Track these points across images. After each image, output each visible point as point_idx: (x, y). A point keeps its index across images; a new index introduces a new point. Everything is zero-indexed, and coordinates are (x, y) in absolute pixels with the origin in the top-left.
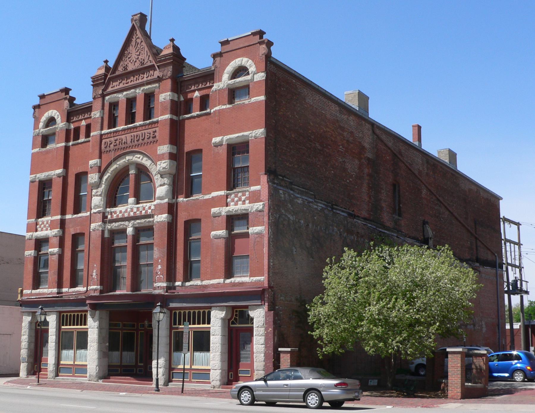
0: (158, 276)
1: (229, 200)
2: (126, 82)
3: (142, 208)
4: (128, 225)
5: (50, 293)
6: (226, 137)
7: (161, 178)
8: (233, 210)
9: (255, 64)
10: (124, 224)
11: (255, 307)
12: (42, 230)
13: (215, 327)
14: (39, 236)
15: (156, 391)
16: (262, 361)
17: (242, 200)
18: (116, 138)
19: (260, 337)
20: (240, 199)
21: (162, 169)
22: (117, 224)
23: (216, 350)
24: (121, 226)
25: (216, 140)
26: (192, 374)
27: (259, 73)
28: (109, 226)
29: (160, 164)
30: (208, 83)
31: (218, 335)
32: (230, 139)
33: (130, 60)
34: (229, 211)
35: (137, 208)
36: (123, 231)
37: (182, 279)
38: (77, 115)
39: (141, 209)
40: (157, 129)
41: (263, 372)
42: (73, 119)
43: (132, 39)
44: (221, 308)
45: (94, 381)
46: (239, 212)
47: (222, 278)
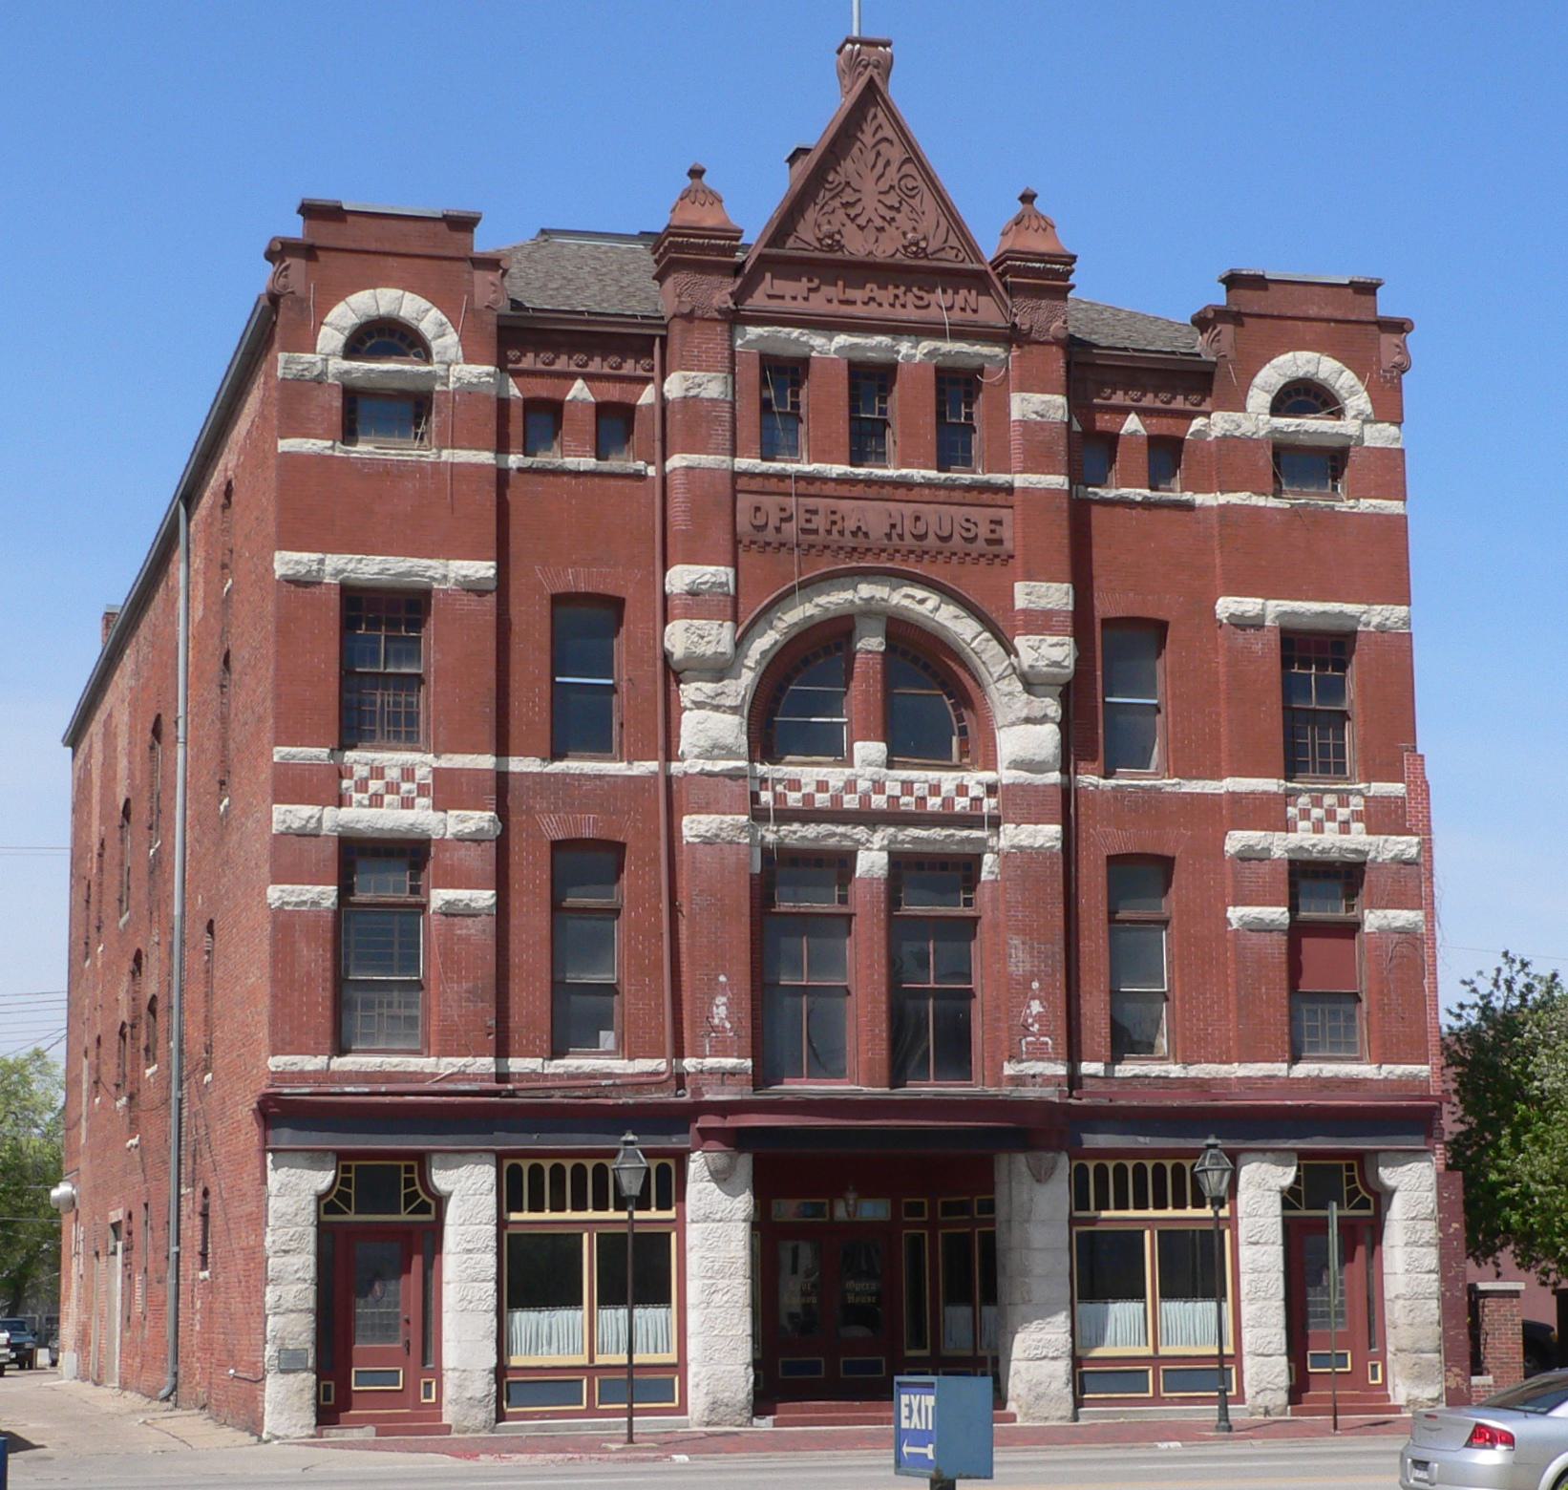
0: (1030, 1039)
1: (1292, 811)
2: (842, 297)
3: (927, 785)
4: (868, 841)
5: (451, 1074)
6: (1278, 606)
7: (1026, 695)
8: (1314, 846)
9: (1367, 389)
10: (844, 836)
11: (1400, 1156)
12: (376, 801)
13: (1260, 1216)
14: (359, 826)
15: (1217, 1428)
16: (1431, 1323)
17: (1340, 818)
18: (811, 503)
19: (1424, 1250)
20: (1331, 815)
21: (1047, 665)
22: (812, 831)
23: (1266, 1292)
24: (832, 842)
25: (1227, 606)
26: (1161, 1373)
27: (1382, 422)
28: (770, 834)
29: (1037, 644)
30: (1180, 398)
31: (1273, 1243)
32: (1294, 614)
33: (853, 212)
34: (1301, 847)
35: (903, 782)
36: (844, 861)
37: (1106, 1052)
39: (920, 789)
40: (1005, 514)
41: (1437, 1355)
42: (518, 361)
43: (859, 134)
44: (1280, 1157)
45: (730, 1425)
46: (1334, 855)
47: (1283, 1061)
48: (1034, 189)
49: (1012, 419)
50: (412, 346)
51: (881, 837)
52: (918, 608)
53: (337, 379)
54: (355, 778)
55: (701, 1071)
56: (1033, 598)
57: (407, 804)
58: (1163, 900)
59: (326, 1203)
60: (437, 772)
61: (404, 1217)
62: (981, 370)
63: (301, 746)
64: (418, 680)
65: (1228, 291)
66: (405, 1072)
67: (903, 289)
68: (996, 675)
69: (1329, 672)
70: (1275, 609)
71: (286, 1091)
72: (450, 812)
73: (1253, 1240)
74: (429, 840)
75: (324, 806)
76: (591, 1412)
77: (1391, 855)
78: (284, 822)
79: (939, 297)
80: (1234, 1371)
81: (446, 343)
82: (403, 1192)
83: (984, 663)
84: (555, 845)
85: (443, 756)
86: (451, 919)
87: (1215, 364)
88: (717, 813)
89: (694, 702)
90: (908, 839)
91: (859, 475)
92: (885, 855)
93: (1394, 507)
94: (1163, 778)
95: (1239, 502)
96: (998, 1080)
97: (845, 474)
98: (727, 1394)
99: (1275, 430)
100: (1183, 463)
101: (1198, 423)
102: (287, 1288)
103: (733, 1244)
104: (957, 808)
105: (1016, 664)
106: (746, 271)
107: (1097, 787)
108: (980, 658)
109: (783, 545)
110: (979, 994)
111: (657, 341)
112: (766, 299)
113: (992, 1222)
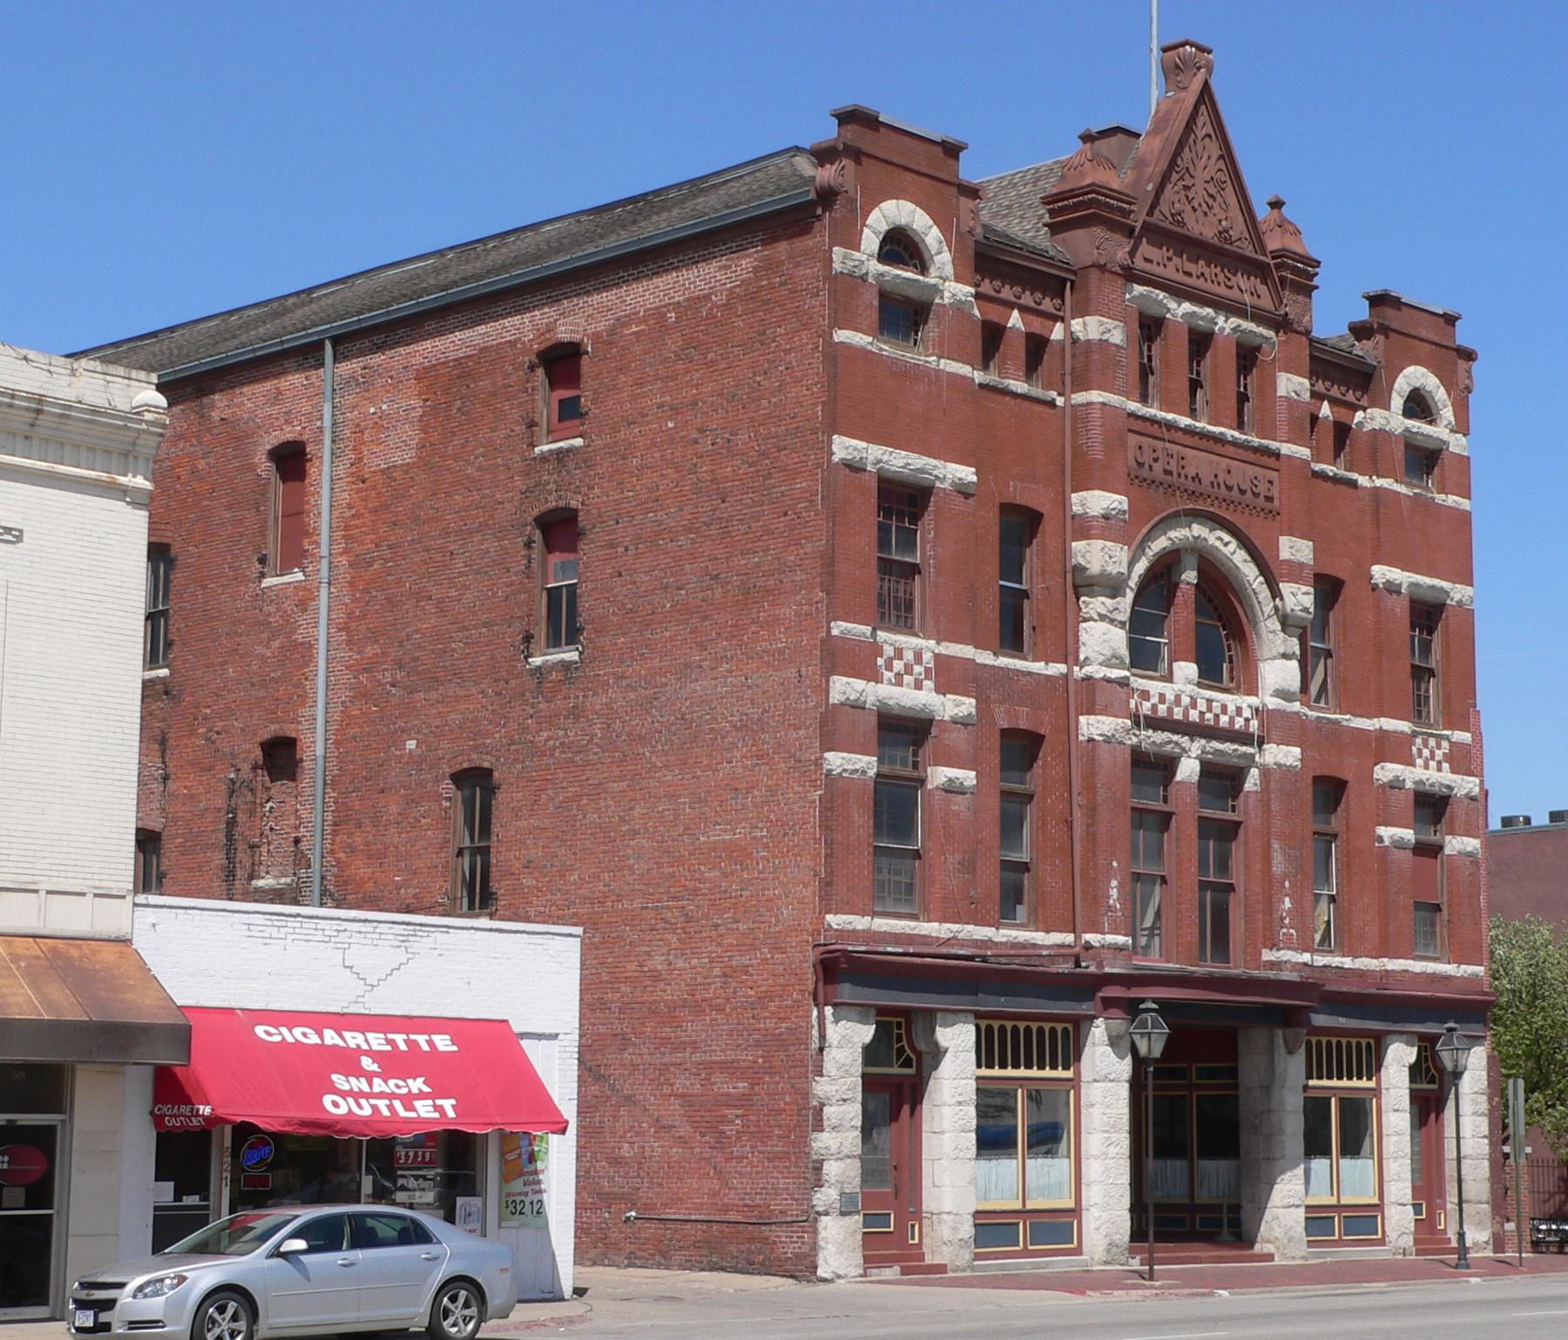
10: (1177, 743)
12: (899, 683)
14: (891, 702)
21: (1301, 610)
24: (1169, 748)
25: (1381, 573)
38: (1018, 284)
39: (1216, 707)
48: (1283, 198)
49: (1278, 394)
50: (912, 257)
51: (1196, 747)
52: (1222, 548)
53: (875, 278)
54: (885, 657)
55: (1103, 946)
56: (1293, 551)
57: (918, 685)
58: (1333, 817)
59: (871, 1054)
60: (938, 657)
61: (896, 1070)
62: (1258, 348)
63: (854, 623)
64: (914, 570)
65: (1370, 307)
66: (918, 935)
67: (1219, 268)
68: (1266, 614)
69: (1424, 636)
70: (1403, 577)
71: (850, 948)
72: (949, 696)
73: (1396, 1108)
74: (931, 721)
75: (869, 681)
76: (1025, 1253)
77: (1466, 791)
78: (845, 693)
79: (1240, 280)
80: (1379, 1218)
81: (943, 261)
82: (896, 1046)
83: (1259, 602)
84: (1003, 730)
85: (943, 644)
86: (951, 796)
87: (1375, 367)
88: (1112, 716)
89: (1099, 615)
90: (1212, 750)
91: (1196, 428)
92: (1197, 762)
93: (1465, 504)
94: (1335, 713)
95: (1387, 486)
96: (1256, 961)
97: (1190, 426)
98: (1118, 1236)
99: (1407, 430)
100: (1347, 447)
101: (1359, 415)
102: (845, 1134)
103: (1121, 1102)
104: (1237, 727)
105: (1280, 606)
106: (1136, 234)
107: (1307, 716)
108: (1257, 598)
109: (1153, 482)
110: (1241, 889)
111: (1069, 284)
112: (1142, 260)
113: (1236, 1087)
